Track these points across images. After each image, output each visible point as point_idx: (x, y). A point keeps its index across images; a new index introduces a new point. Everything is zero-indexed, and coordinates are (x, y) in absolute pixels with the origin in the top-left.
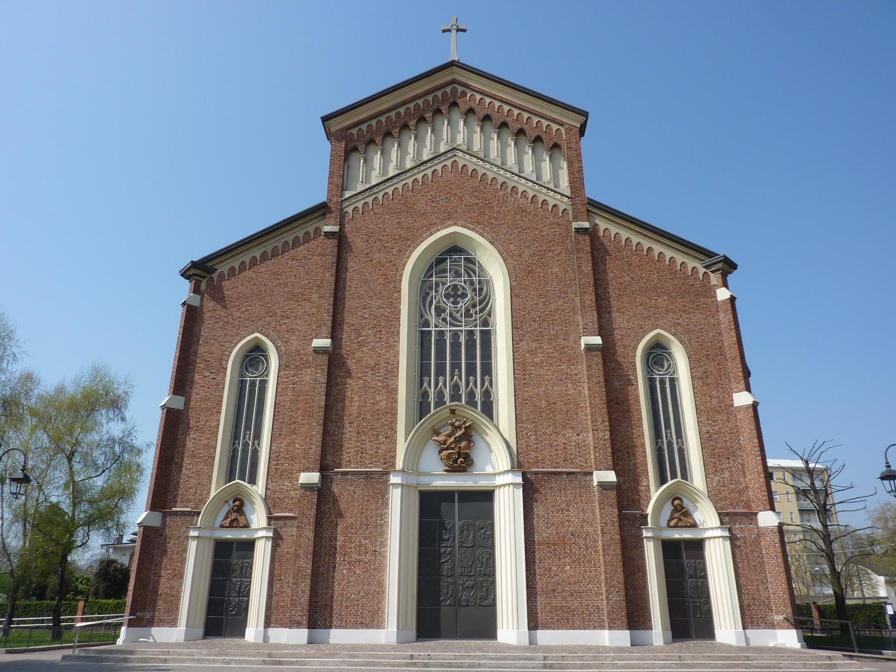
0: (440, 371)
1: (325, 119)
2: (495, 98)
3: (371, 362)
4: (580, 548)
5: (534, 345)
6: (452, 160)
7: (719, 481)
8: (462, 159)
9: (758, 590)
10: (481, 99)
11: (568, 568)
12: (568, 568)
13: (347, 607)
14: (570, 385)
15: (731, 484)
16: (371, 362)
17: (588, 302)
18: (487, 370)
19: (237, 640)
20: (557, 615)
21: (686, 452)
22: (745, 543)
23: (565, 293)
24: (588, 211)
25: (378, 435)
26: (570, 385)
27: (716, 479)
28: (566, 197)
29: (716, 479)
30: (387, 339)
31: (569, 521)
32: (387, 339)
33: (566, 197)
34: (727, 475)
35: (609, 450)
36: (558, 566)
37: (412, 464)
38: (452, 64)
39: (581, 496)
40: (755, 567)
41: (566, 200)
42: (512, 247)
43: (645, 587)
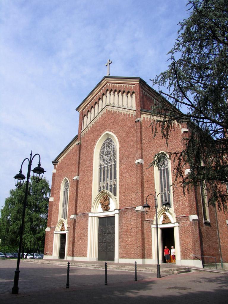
0: (104, 180)
1: (77, 110)
2: (97, 93)
3: (87, 181)
4: (133, 233)
5: (125, 166)
6: (106, 110)
7: (178, 205)
8: (109, 108)
9: (188, 245)
10: (114, 85)
11: (130, 239)
12: (130, 239)
13: (81, 251)
14: (134, 178)
15: (182, 206)
16: (87, 181)
17: (138, 147)
18: (115, 177)
19: (63, 259)
20: (126, 254)
21: (170, 196)
22: (184, 228)
23: (134, 146)
24: (141, 113)
25: (88, 202)
26: (134, 178)
27: (178, 204)
28: (135, 110)
29: (178, 204)
30: (90, 173)
31: (130, 224)
32: (90, 173)
33: (135, 110)
34: (181, 202)
35: (141, 199)
36: (127, 239)
37: (97, 211)
38: (105, 77)
39: (134, 216)
40: (187, 237)
41: (135, 111)
42: (120, 133)
43: (114, 247)
